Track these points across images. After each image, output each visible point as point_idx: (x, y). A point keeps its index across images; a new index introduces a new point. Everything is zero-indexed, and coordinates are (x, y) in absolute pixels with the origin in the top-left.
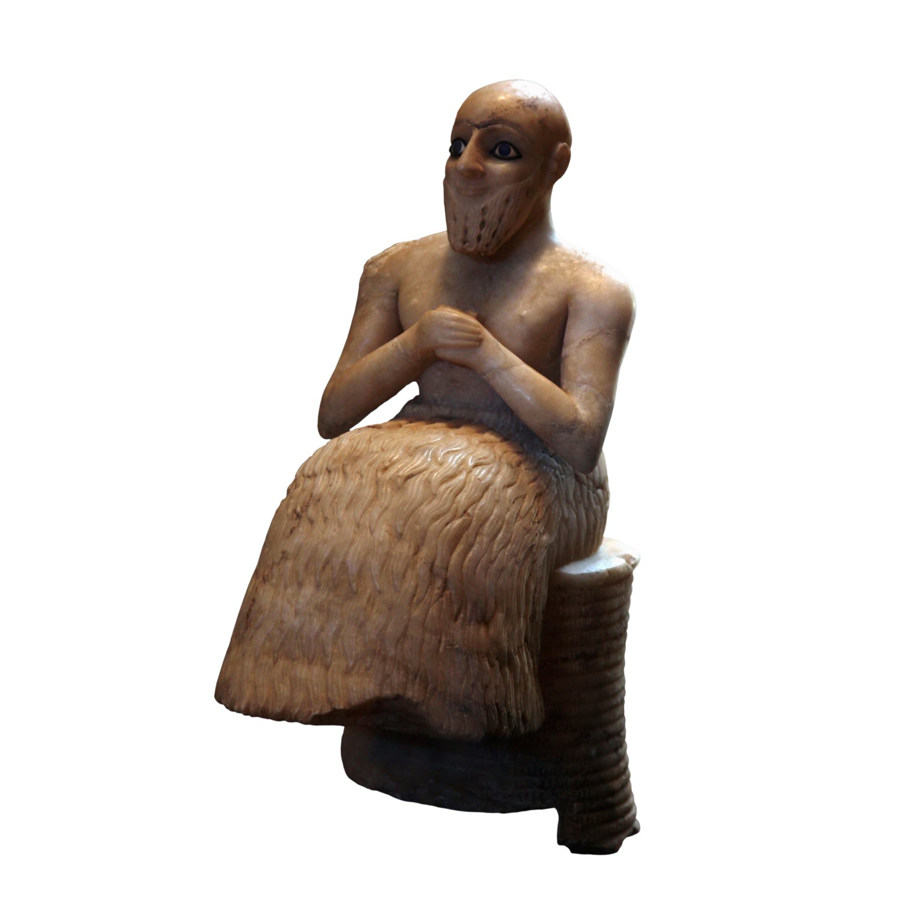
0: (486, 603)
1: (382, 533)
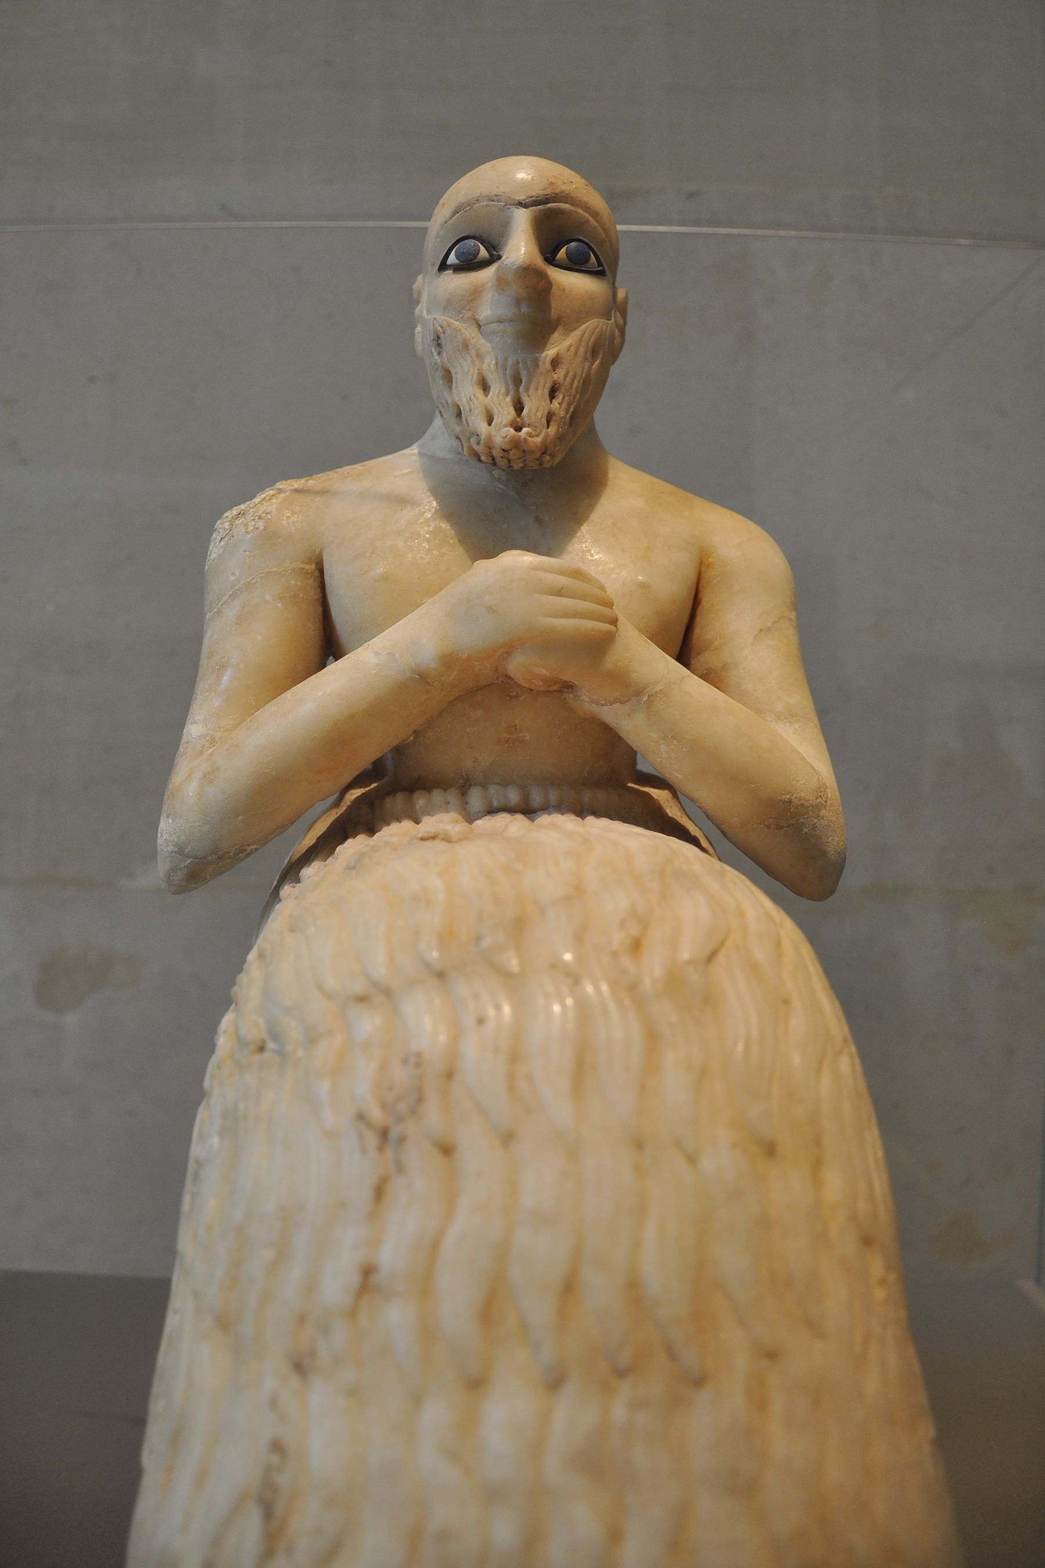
1: (722, 1159)
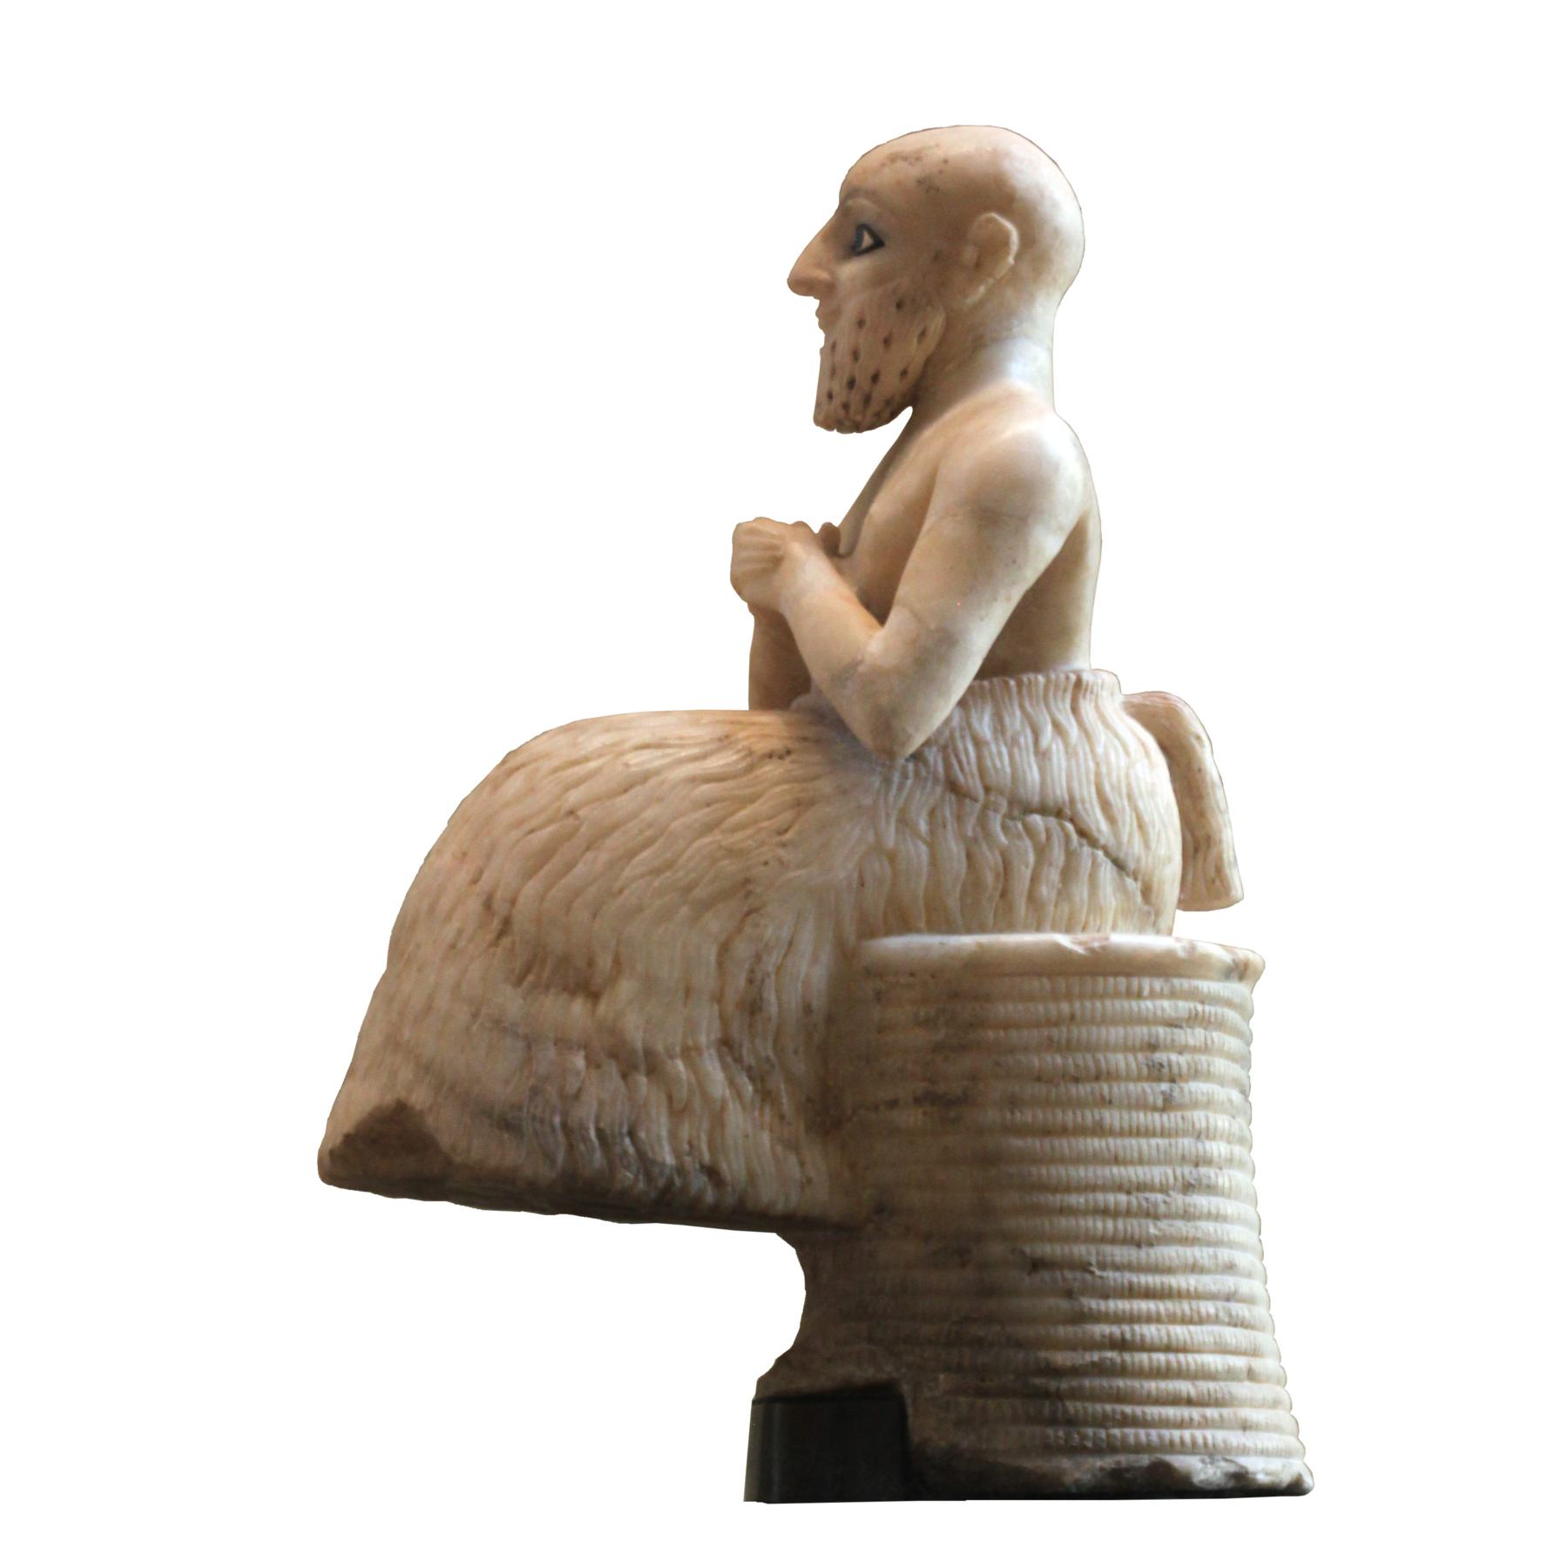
0: (591, 963)
